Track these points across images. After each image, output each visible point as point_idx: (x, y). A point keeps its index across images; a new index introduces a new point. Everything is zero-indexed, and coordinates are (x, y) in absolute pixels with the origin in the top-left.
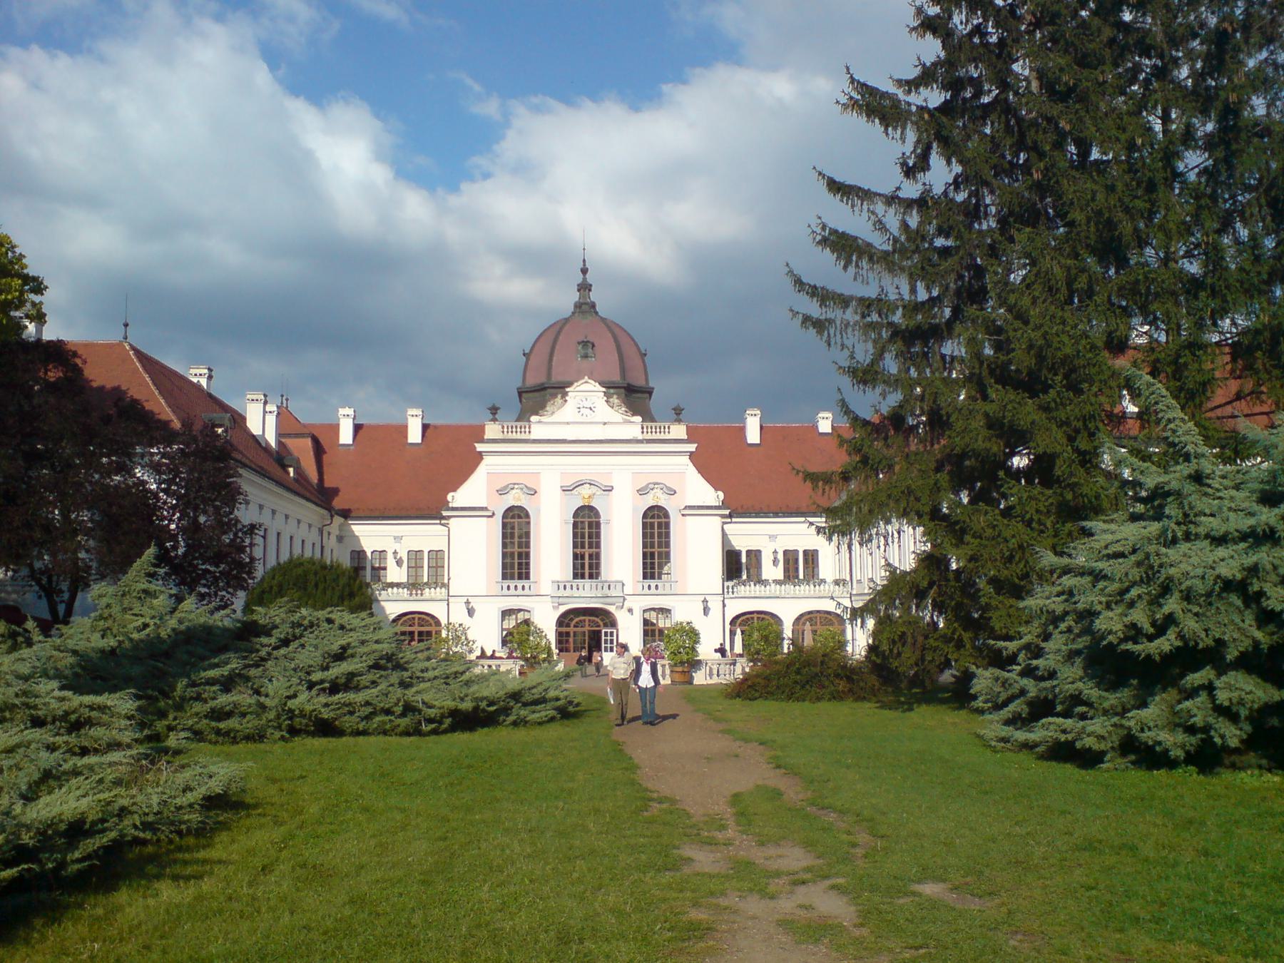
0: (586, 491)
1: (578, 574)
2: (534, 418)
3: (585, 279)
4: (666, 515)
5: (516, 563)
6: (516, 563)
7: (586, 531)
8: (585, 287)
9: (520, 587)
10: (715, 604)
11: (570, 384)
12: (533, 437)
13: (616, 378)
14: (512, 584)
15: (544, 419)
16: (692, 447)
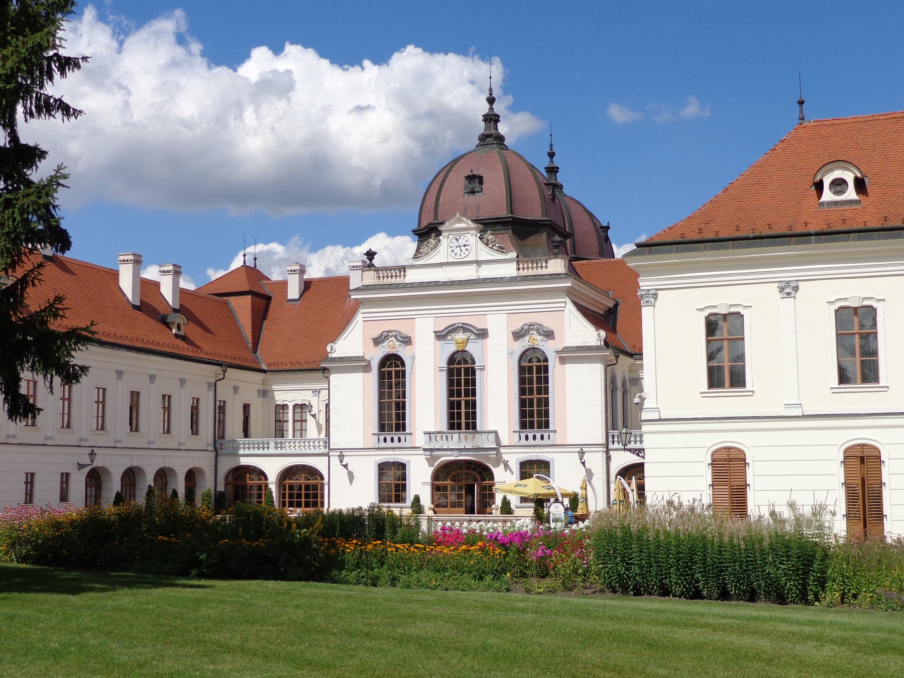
0: (460, 336)
1: (454, 424)
3: (491, 109)
5: (392, 417)
6: (392, 417)
7: (461, 378)
9: (396, 438)
13: (503, 213)
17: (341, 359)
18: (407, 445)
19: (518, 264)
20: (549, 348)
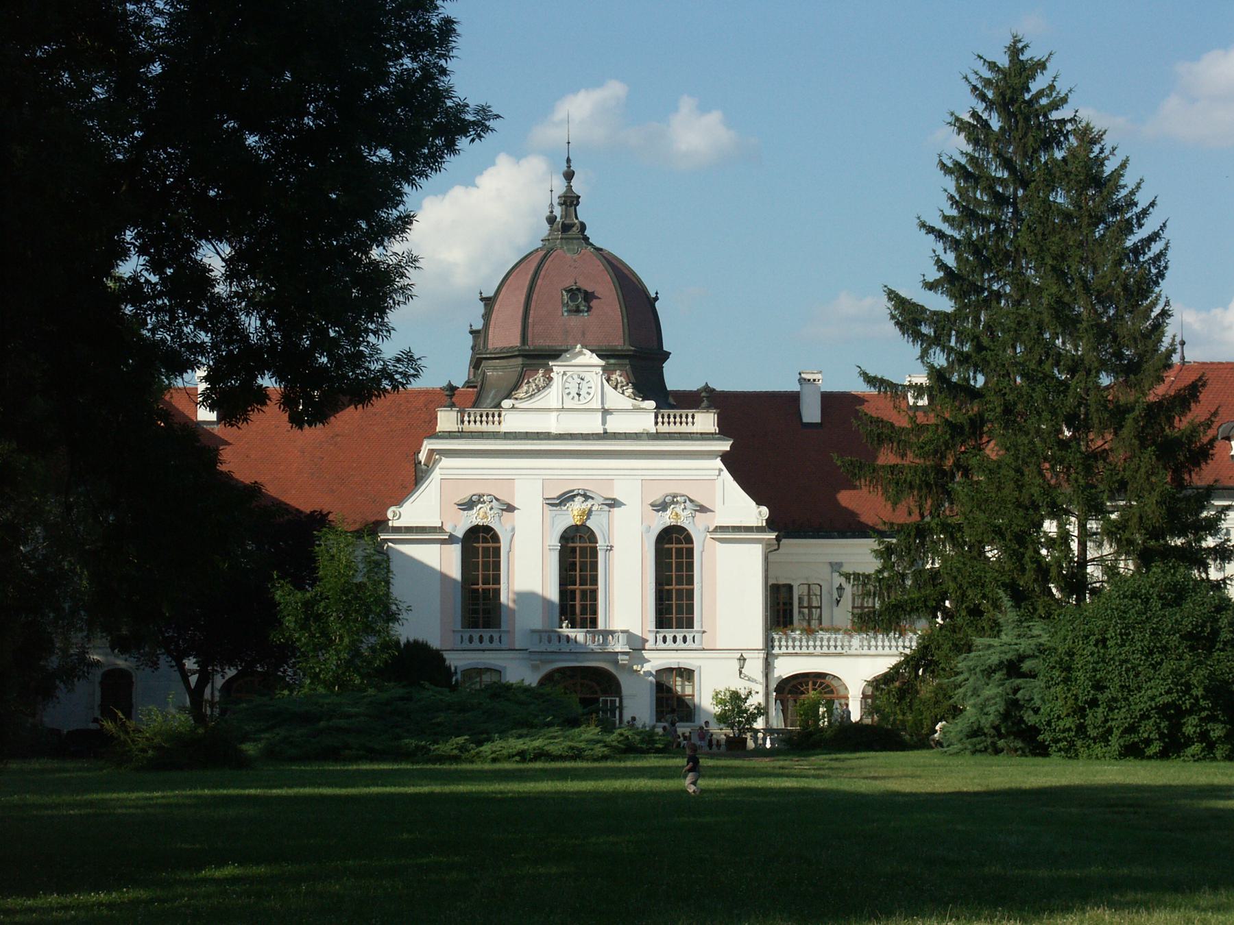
0: (577, 506)
2: (506, 403)
3: (569, 187)
4: (689, 540)
8: (570, 201)
10: (755, 666)
11: (556, 355)
12: (504, 428)
14: (476, 634)
15: (518, 404)
16: (726, 446)
17: (409, 530)
18: (503, 647)
19: (656, 417)
20: (697, 528)
